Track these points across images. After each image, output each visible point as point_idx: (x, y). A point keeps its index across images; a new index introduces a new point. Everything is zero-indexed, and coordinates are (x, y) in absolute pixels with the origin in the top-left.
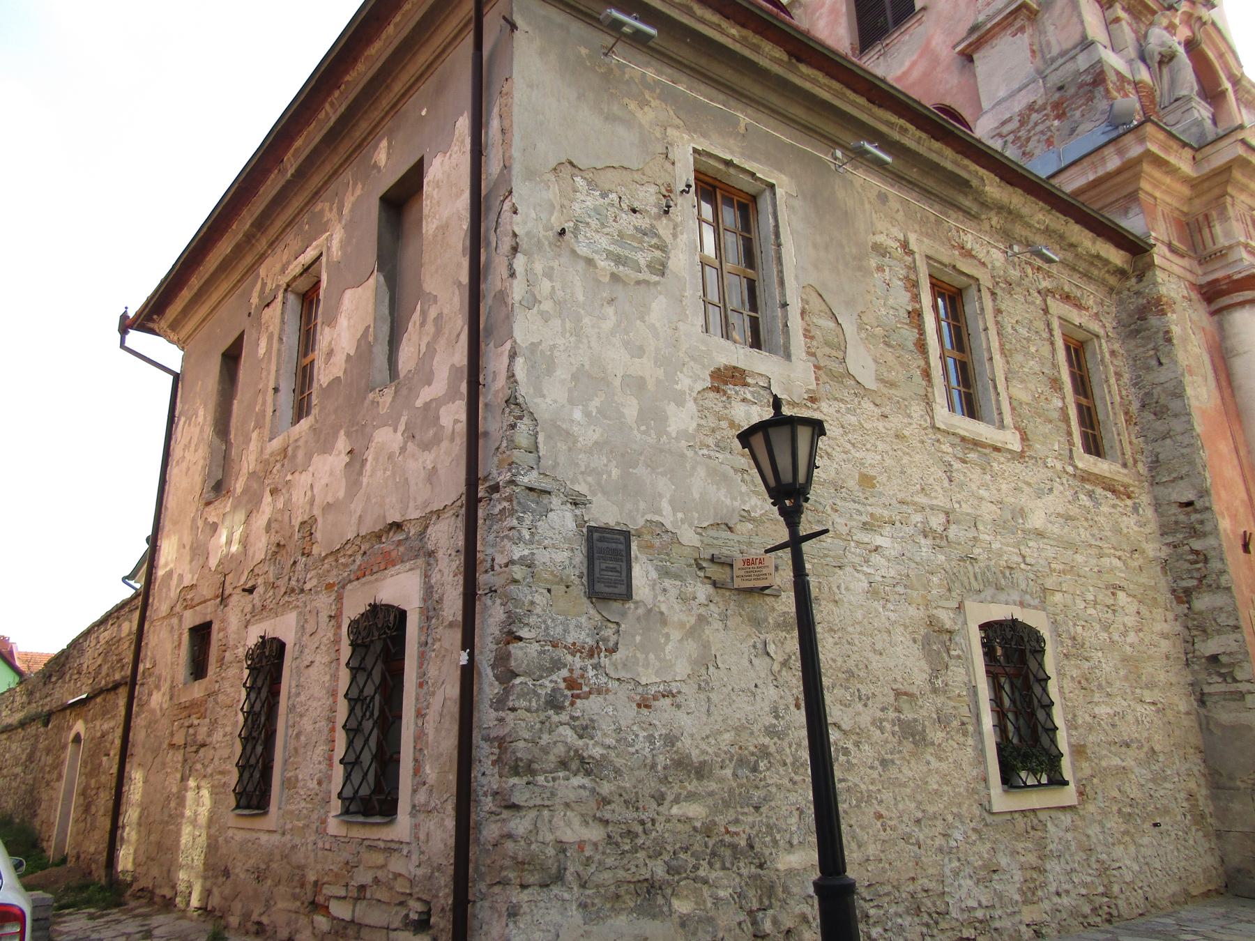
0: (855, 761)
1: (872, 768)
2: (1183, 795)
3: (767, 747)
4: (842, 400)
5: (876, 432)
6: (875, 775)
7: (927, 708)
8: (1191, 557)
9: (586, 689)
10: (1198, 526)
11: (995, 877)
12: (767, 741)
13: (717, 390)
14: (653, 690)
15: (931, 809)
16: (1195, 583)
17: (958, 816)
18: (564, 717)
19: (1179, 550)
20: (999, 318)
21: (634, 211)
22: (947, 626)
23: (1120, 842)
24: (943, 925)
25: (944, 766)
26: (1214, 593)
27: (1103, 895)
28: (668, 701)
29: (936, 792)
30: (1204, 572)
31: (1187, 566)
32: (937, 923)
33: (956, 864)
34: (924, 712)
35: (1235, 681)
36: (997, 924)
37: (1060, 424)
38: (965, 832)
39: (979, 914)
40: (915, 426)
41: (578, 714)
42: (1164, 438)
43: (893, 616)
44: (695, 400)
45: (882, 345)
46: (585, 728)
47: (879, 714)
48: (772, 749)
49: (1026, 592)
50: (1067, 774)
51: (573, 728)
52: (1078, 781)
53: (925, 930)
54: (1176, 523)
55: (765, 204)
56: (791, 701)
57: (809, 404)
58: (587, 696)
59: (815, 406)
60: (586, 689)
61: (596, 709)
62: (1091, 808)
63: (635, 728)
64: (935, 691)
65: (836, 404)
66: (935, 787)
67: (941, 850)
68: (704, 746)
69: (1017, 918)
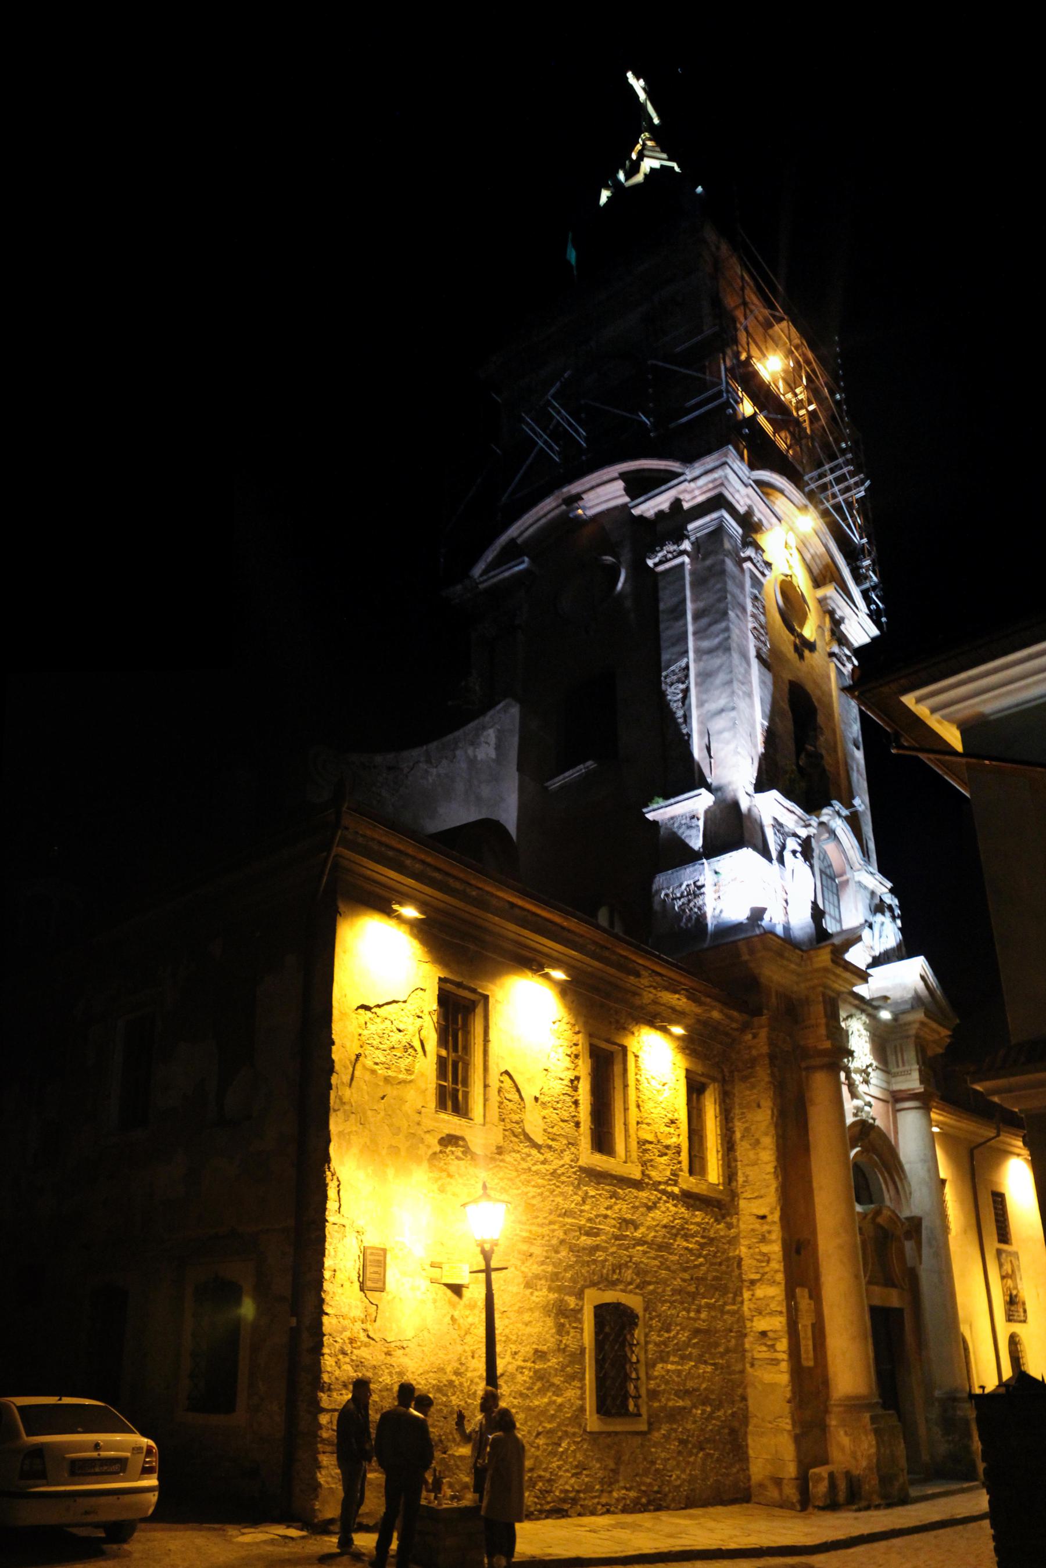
0: (504, 1393)
1: (515, 1398)
2: (726, 1431)
3: (454, 1381)
4: (519, 1152)
5: (537, 1173)
6: (516, 1402)
7: (553, 1362)
8: (759, 1257)
9: (359, 1344)
10: (767, 1235)
11: (585, 1472)
12: (454, 1378)
13: (441, 1152)
14: (393, 1345)
15: (548, 1426)
16: (757, 1277)
17: (566, 1432)
18: (347, 1359)
19: (751, 1251)
20: (638, 1077)
21: (400, 1031)
22: (572, 1306)
23: (674, 1458)
24: (549, 1499)
25: (559, 1400)
26: (771, 1286)
27: (657, 1492)
28: (401, 1352)
29: (553, 1415)
30: (767, 1269)
31: (755, 1263)
32: (545, 1498)
33: (561, 1463)
34: (550, 1364)
35: (776, 1351)
36: (582, 1503)
37: (673, 1156)
38: (569, 1443)
39: (572, 1495)
40: (567, 1166)
41: (354, 1358)
42: (753, 1165)
43: (537, 1300)
44: (429, 1160)
45: (552, 1110)
46: (357, 1366)
47: (523, 1364)
48: (457, 1383)
49: (630, 1283)
50: (644, 1411)
51: (352, 1366)
52: (650, 1416)
53: (536, 1500)
54: (753, 1230)
55: (479, 1011)
56: (470, 1354)
57: (497, 1156)
58: (359, 1348)
59: (501, 1157)
60: (359, 1344)
61: (364, 1355)
62: (656, 1434)
63: (383, 1367)
64: (559, 1350)
65: (514, 1154)
66: (552, 1412)
67: (550, 1453)
68: (420, 1380)
69: (596, 1501)
